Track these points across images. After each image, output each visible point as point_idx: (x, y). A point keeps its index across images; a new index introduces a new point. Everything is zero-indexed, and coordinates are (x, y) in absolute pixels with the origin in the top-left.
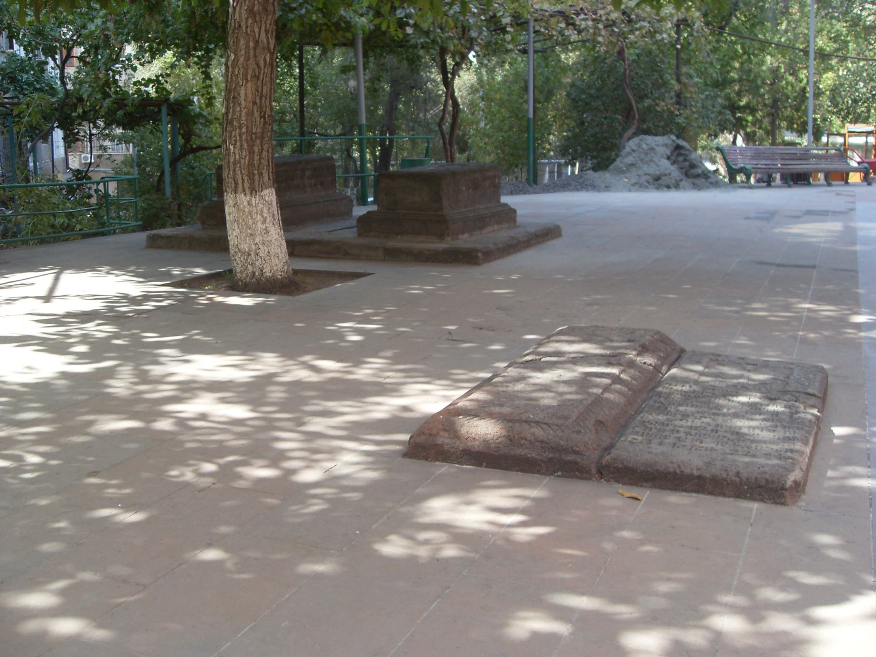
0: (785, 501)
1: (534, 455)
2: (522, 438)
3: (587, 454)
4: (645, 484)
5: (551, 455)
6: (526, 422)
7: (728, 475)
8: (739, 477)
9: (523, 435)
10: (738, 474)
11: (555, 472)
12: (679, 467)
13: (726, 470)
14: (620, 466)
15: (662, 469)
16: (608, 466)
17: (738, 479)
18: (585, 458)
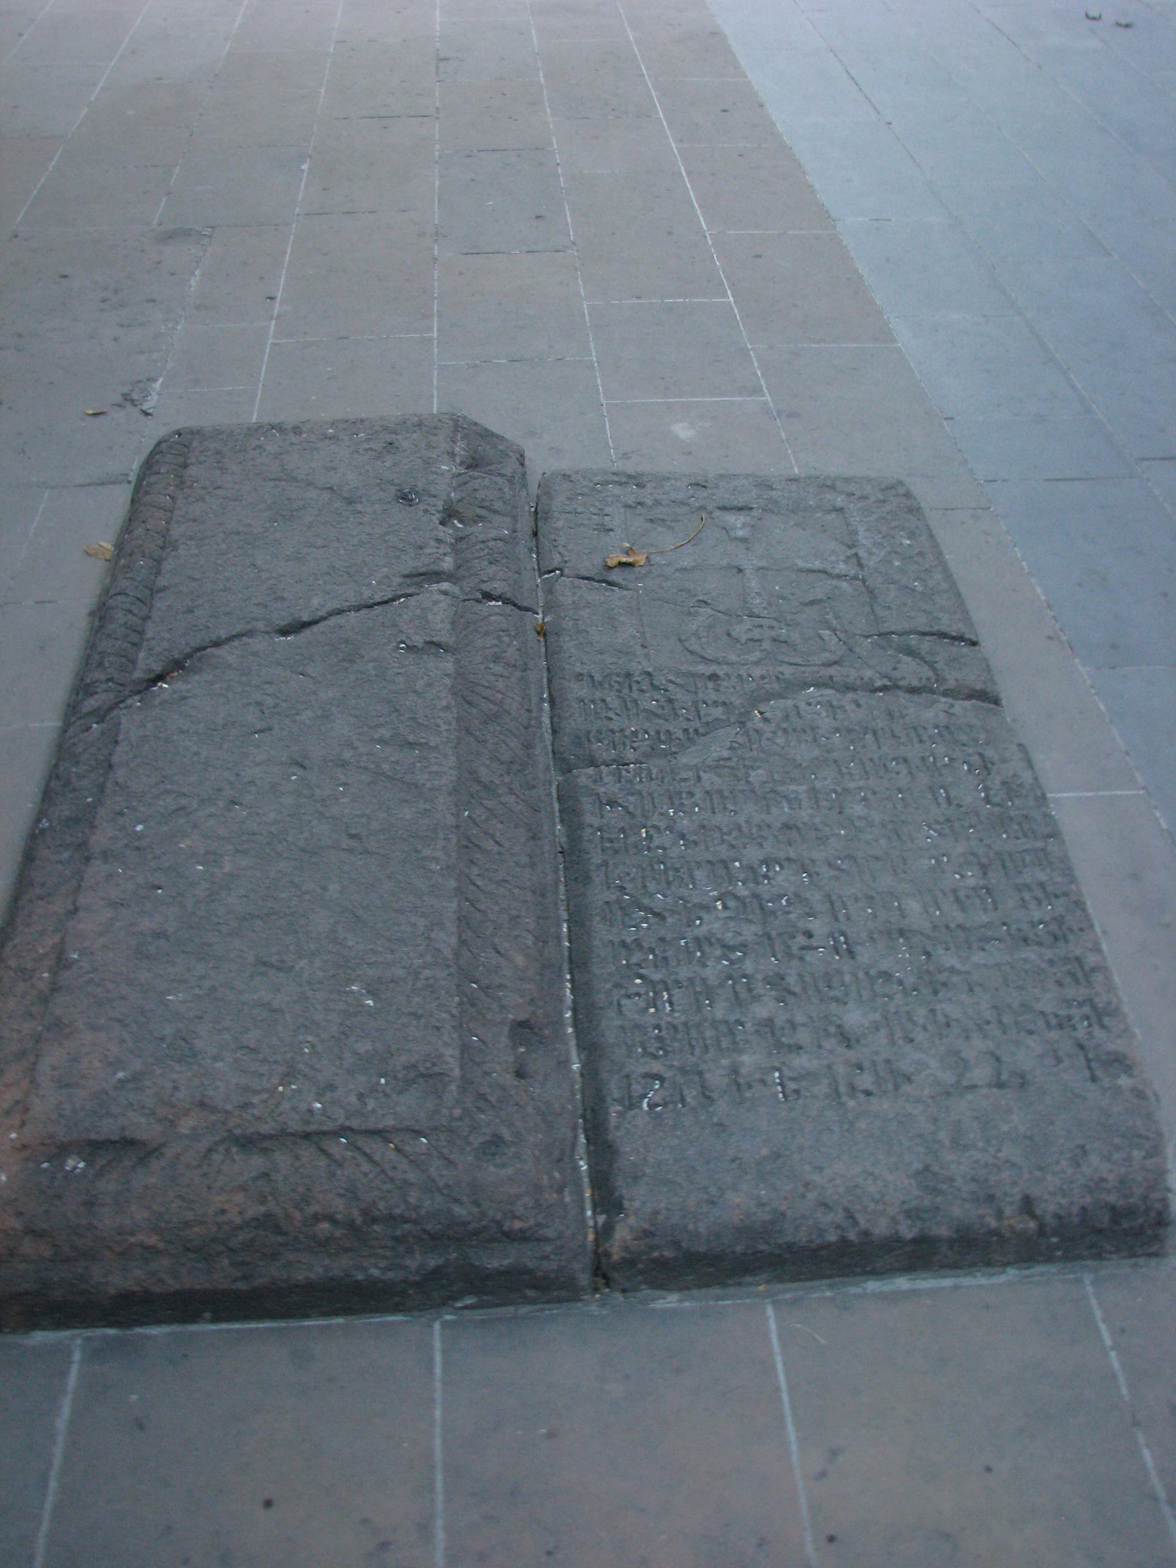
1: (375, 1272)
2: (317, 1218)
3: (550, 1233)
4: (748, 1279)
5: (433, 1262)
6: (307, 1136)
7: (1000, 1215)
8: (1032, 1215)
9: (314, 1208)
10: (1028, 1205)
11: (455, 1298)
12: (849, 1215)
13: (991, 1198)
14: (668, 1253)
15: (802, 1237)
16: (629, 1263)
17: (1032, 1225)
18: (548, 1248)
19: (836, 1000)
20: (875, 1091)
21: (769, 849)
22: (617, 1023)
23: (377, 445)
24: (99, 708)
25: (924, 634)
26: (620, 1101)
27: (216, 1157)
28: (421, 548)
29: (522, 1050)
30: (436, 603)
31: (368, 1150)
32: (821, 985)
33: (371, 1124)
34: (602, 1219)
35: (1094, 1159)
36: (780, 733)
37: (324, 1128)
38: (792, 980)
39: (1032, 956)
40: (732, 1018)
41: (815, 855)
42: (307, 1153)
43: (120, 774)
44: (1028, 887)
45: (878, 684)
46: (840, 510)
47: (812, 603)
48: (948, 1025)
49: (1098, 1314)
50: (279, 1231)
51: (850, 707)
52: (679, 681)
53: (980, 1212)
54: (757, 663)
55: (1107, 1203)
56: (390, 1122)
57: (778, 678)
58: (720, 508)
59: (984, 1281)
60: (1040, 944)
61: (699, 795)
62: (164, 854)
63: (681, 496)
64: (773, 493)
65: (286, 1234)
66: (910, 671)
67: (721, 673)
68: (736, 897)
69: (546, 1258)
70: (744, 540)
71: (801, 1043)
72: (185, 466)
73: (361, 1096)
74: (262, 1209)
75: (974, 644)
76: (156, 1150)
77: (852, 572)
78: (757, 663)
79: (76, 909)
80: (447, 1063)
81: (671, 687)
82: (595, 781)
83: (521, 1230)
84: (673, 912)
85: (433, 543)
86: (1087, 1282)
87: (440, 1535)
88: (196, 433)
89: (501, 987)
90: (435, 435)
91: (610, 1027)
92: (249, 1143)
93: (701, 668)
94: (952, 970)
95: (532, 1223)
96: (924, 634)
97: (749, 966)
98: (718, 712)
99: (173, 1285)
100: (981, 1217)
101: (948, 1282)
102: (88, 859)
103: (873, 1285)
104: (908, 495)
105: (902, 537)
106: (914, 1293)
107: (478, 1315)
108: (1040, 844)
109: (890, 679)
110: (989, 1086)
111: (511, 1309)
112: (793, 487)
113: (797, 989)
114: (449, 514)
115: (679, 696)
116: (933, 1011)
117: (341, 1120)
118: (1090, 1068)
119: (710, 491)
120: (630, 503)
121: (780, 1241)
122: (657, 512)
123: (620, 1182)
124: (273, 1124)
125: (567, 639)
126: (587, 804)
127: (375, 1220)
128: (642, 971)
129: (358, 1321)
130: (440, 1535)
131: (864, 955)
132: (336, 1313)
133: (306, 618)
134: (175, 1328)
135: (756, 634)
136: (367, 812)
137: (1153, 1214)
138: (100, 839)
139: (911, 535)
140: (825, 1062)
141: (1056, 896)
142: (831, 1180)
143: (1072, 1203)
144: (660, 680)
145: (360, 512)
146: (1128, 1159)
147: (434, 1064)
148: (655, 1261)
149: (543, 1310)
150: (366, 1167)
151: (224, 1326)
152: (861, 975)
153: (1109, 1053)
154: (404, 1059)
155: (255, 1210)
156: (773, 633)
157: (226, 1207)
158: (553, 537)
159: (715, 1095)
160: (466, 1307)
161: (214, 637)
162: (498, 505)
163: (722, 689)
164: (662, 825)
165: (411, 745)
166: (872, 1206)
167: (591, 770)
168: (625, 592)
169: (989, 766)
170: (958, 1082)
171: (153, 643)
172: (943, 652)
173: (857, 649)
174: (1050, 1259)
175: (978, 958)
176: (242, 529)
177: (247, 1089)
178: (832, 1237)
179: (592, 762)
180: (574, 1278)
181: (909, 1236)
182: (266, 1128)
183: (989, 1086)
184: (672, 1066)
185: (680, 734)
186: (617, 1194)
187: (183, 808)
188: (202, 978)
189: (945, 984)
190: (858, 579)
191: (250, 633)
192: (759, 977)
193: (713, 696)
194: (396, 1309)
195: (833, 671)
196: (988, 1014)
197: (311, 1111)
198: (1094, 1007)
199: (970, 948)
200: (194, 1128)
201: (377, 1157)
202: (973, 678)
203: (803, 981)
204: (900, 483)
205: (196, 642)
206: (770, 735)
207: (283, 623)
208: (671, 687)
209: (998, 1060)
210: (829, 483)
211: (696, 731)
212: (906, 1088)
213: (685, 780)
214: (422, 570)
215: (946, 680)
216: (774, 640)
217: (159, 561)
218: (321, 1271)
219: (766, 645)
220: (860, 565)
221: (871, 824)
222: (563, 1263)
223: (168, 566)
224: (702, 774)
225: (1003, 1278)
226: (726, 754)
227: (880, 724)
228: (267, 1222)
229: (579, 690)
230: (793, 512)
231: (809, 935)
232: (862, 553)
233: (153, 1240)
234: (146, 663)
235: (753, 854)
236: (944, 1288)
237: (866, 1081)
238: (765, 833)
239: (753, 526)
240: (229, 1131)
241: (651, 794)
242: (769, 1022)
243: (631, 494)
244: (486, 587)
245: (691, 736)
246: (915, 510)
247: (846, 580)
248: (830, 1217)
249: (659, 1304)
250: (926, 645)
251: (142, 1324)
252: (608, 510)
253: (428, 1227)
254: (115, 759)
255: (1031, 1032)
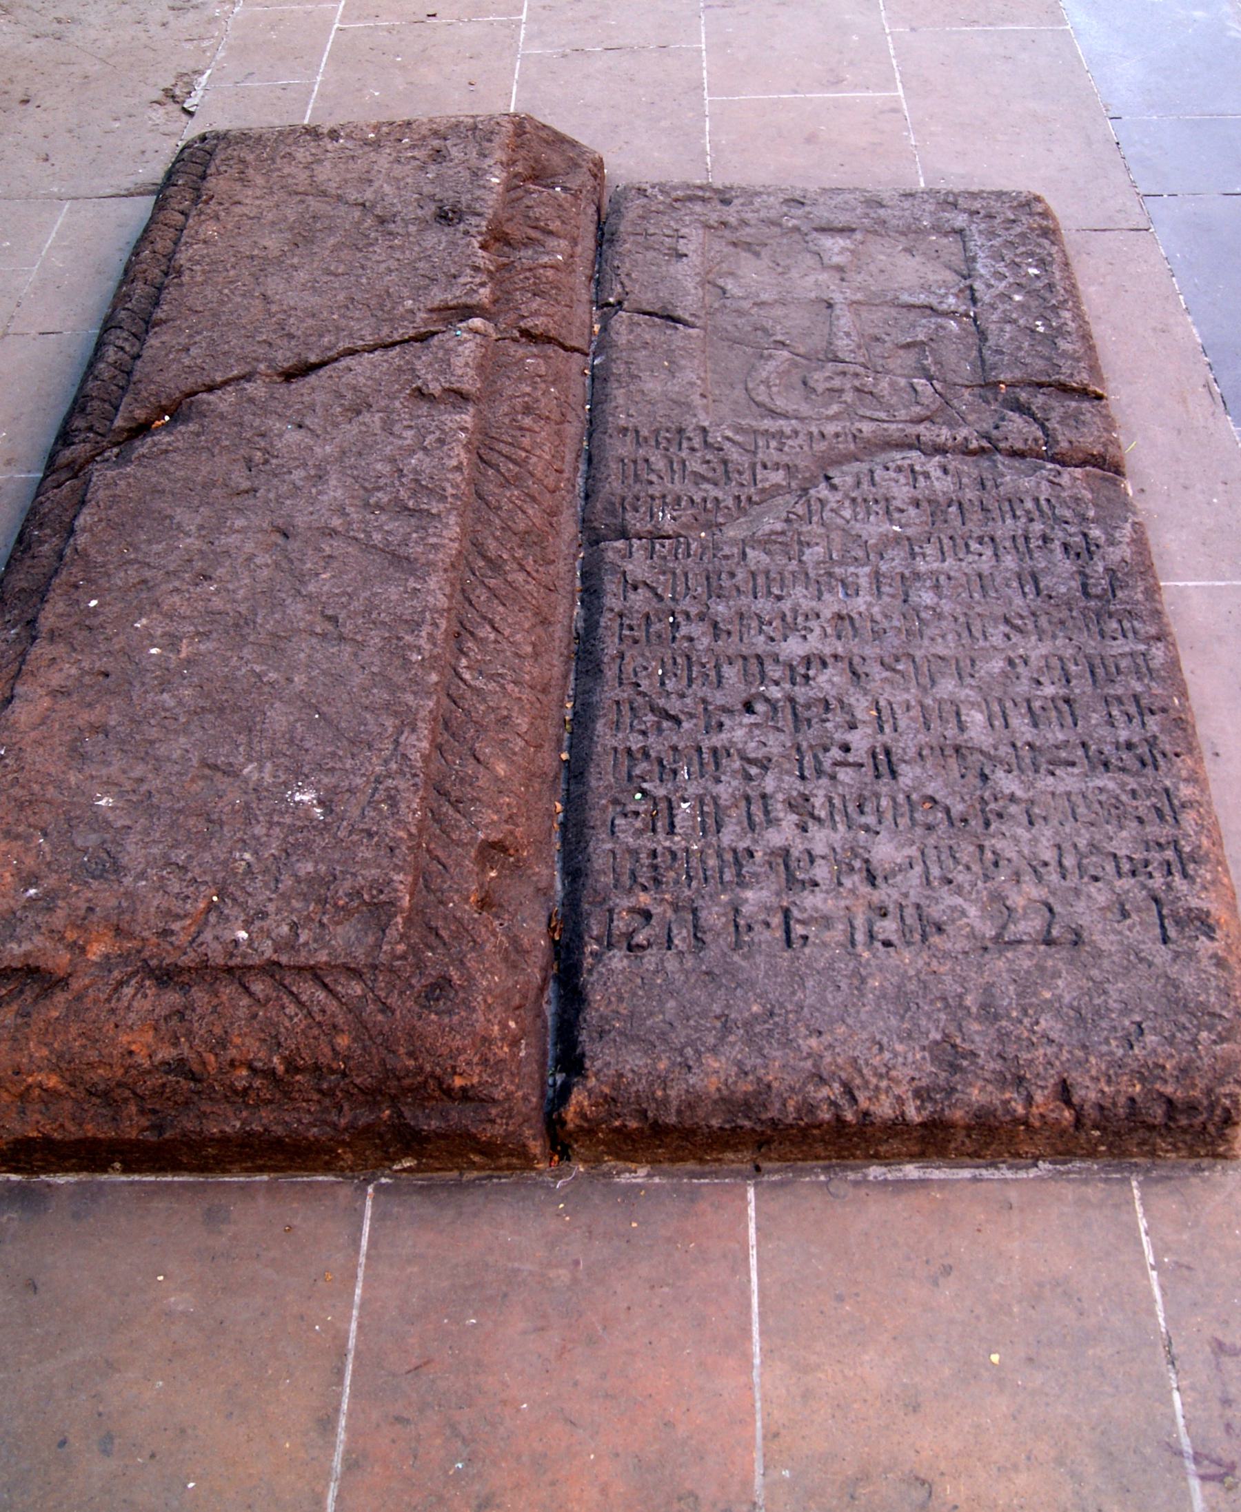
0: (1231, 1149)
3: (498, 1094)
6: (229, 970)
7: (1029, 1100)
8: (1068, 1102)
9: (233, 1053)
12: (849, 1091)
13: (1020, 1080)
14: (633, 1124)
16: (588, 1130)
17: (1067, 1114)
18: (494, 1111)
19: (867, 829)
20: (896, 942)
21: (814, 643)
22: (609, 846)
23: (421, 154)
24: (74, 462)
25: (1040, 385)
26: (598, 940)
27: (128, 991)
28: (455, 277)
29: (493, 874)
30: (461, 343)
31: (294, 989)
32: (851, 808)
33: (302, 959)
34: (560, 1078)
35: (1151, 1039)
36: (847, 503)
37: (249, 962)
38: (818, 801)
39: (1111, 785)
40: (742, 845)
41: (871, 651)
42: (228, 991)
43: (82, 540)
44: (1119, 700)
45: (974, 445)
46: (960, 232)
47: (908, 346)
48: (996, 864)
49: (1143, 1224)
50: (192, 1076)
51: (936, 473)
52: (738, 438)
53: (1007, 1095)
54: (831, 418)
55: (1161, 1095)
56: (323, 957)
57: (855, 437)
58: (816, 230)
59: (1009, 1175)
60: (1123, 770)
61: (741, 575)
62: (117, 634)
63: (773, 214)
64: (882, 212)
65: (199, 1081)
66: (1018, 429)
67: (788, 431)
68: (767, 700)
69: (493, 1122)
70: (840, 269)
71: (818, 879)
72: (203, 177)
73: (294, 926)
74: (174, 1052)
75: (1099, 397)
76: (61, 980)
77: (962, 309)
78: (831, 418)
79: (12, 697)
80: (396, 890)
81: (727, 445)
82: (623, 557)
83: (464, 1089)
84: (691, 716)
85: (468, 271)
86: (1134, 1184)
87: (342, 1436)
88: (222, 137)
89: (474, 800)
90: (490, 141)
91: (601, 848)
92: (166, 977)
93: (768, 424)
94: (1012, 798)
95: (475, 1080)
96: (1040, 385)
97: (769, 784)
98: (778, 477)
99: (74, 1131)
100: (1008, 1102)
101: (966, 1173)
102: (34, 638)
103: (875, 1172)
104: (1046, 214)
105: (1029, 265)
106: (924, 1183)
107: (419, 1180)
108: (1142, 647)
109: (989, 439)
110: (1035, 942)
111: (455, 1174)
112: (906, 204)
113: (823, 814)
114: (498, 238)
115: (735, 456)
116: (981, 848)
117: (269, 953)
118: (1162, 926)
119: (807, 209)
120: (712, 222)
121: (764, 1117)
122: (745, 234)
123: (583, 1037)
124: (193, 955)
125: (616, 385)
126: (611, 585)
127: (298, 1070)
128: (645, 785)
129: (284, 1179)
130: (342, 1436)
131: (908, 774)
132: (261, 1169)
133: (313, 359)
134: (84, 1176)
135: (837, 383)
136: (349, 590)
137: (1219, 1112)
138: (49, 617)
139: (1042, 263)
140: (843, 903)
141: (1152, 712)
142: (830, 1046)
143: (1118, 1092)
144: (716, 437)
145: (390, 233)
146: (1194, 1042)
147: (381, 892)
148: (617, 1130)
149: (490, 1177)
150: (291, 1009)
151: (136, 1177)
152: (901, 798)
153: (1190, 910)
154: (347, 885)
155: (166, 1053)
156: (857, 383)
157: (133, 1047)
158: (616, 263)
159: (708, 938)
160: (404, 1170)
161: (208, 381)
162: (555, 225)
163: (786, 449)
164: (693, 611)
165: (412, 512)
166: (874, 1081)
167: (620, 544)
168: (691, 331)
169: (1093, 548)
170: (999, 936)
171: (140, 386)
172: (1058, 409)
173: (955, 402)
174: (1092, 1154)
175: (1046, 783)
176: (256, 252)
177: (169, 912)
178: (825, 1115)
179: (624, 534)
180: (524, 1146)
181: (918, 1119)
182: (184, 961)
183: (1035, 942)
184: (663, 900)
185: (730, 502)
186: (579, 1050)
187: (144, 582)
188: (141, 780)
189: (1000, 816)
190: (968, 316)
191: (248, 377)
192: (780, 797)
193: (776, 456)
194: (327, 1168)
195: (921, 429)
196: (1049, 855)
197: (236, 942)
198: (1178, 851)
199: (1037, 771)
200: (107, 957)
201: (304, 998)
202: (1089, 440)
203: (832, 805)
204: (1038, 199)
205: (189, 383)
206: (835, 505)
207: (286, 365)
208: (727, 445)
209: (1051, 910)
210: (951, 199)
211: (749, 499)
212: (935, 939)
213: (726, 557)
214: (451, 304)
215: (1057, 442)
216: (857, 390)
217: (160, 289)
218: (238, 1124)
219: (849, 397)
220: (974, 301)
221: (939, 616)
222: (511, 1128)
223: (170, 294)
224: (748, 550)
225: (1033, 1173)
226: (779, 526)
227: (970, 494)
228: (180, 1067)
229: (621, 448)
230: (903, 234)
231: (846, 748)
232: (978, 285)
233: (53, 1081)
234: (129, 412)
235: (793, 648)
236: (958, 1181)
237: (887, 928)
238: (810, 624)
239: (852, 252)
240: (145, 961)
241: (686, 575)
242: (786, 852)
243: (714, 213)
244: (527, 324)
245: (743, 505)
246: (1050, 233)
247: (954, 319)
248: (825, 1091)
249: (625, 1179)
250: (1039, 401)
251: (46, 1171)
252: (684, 231)
253: (358, 1081)
254: (80, 522)
255: (1096, 879)
